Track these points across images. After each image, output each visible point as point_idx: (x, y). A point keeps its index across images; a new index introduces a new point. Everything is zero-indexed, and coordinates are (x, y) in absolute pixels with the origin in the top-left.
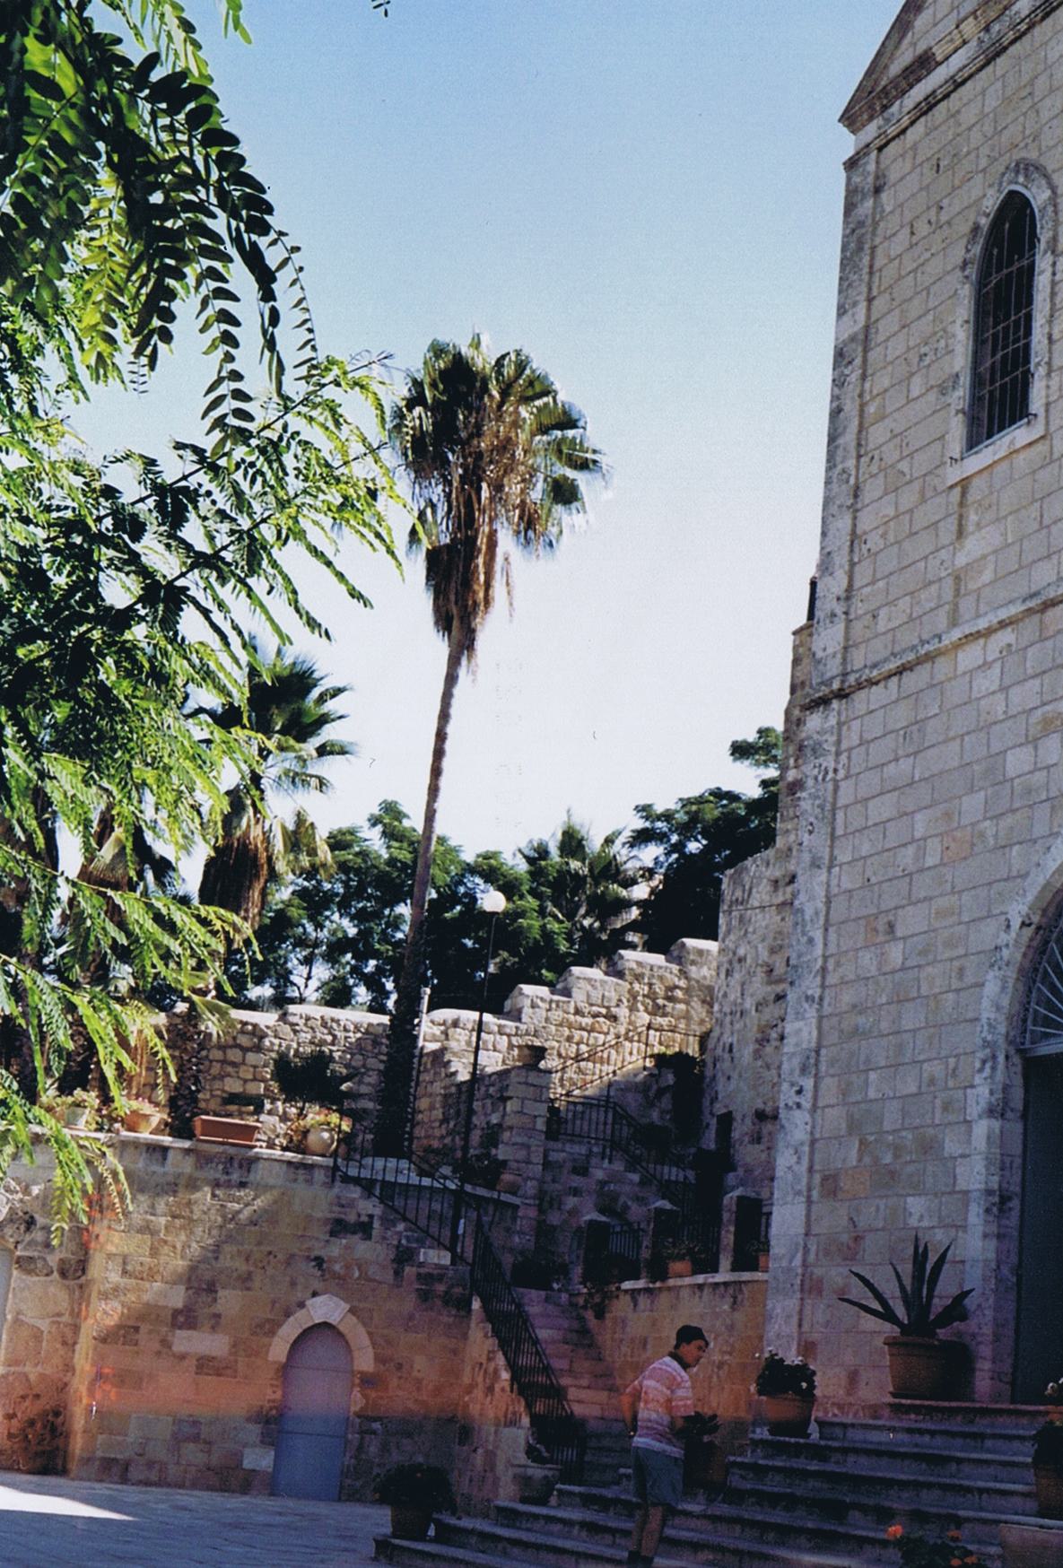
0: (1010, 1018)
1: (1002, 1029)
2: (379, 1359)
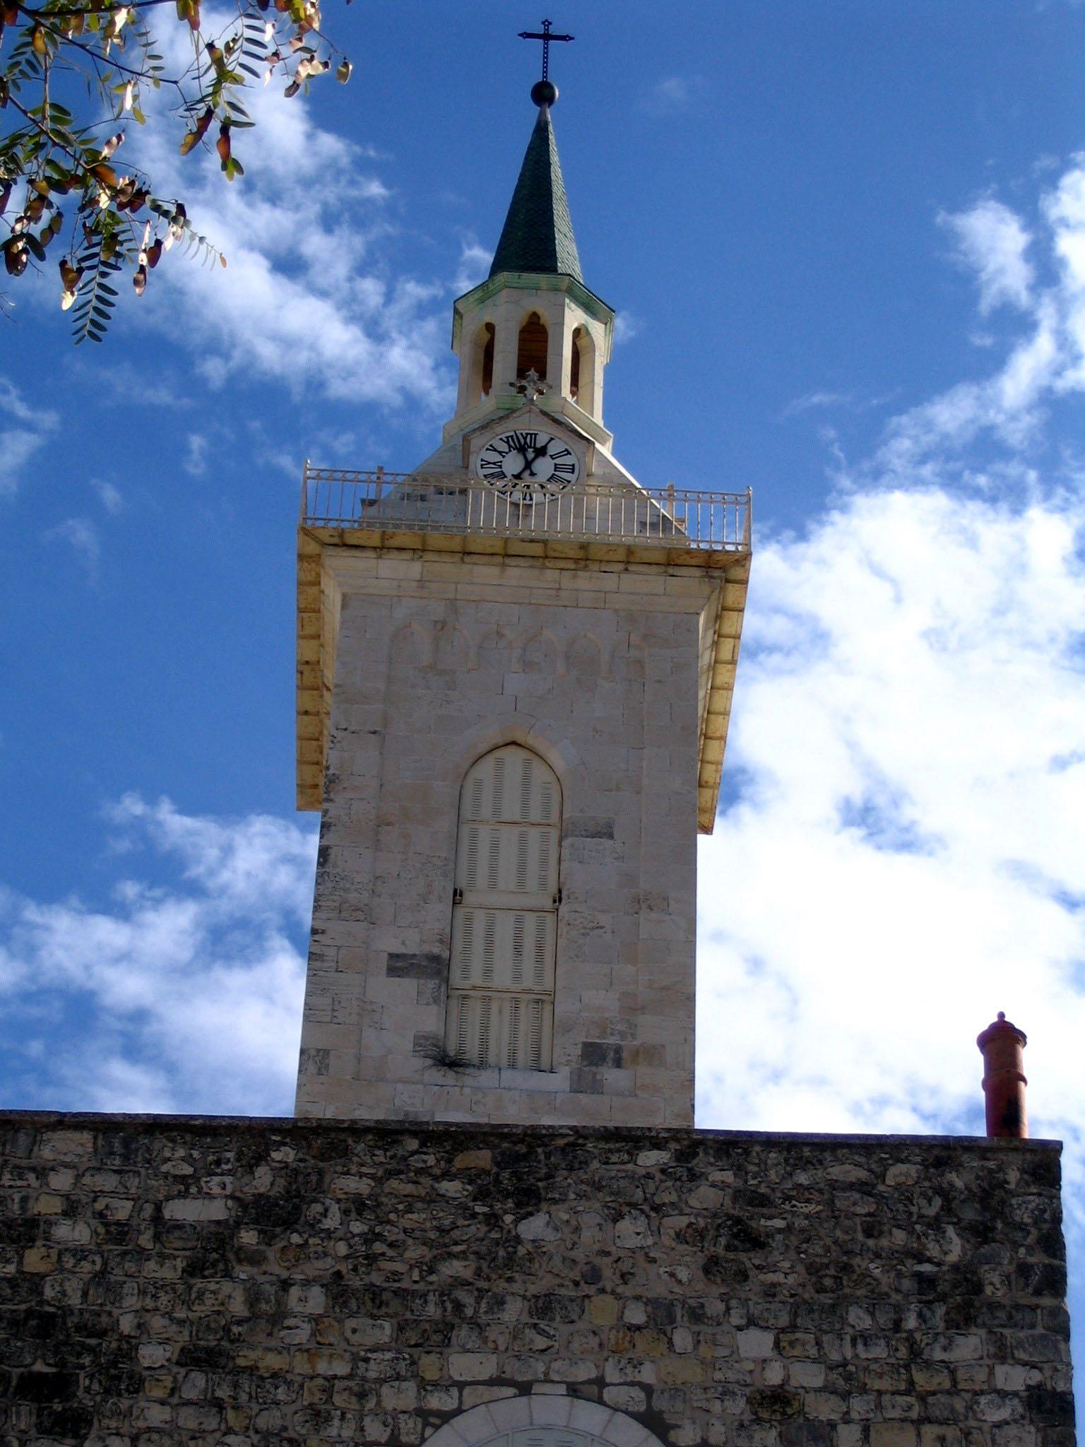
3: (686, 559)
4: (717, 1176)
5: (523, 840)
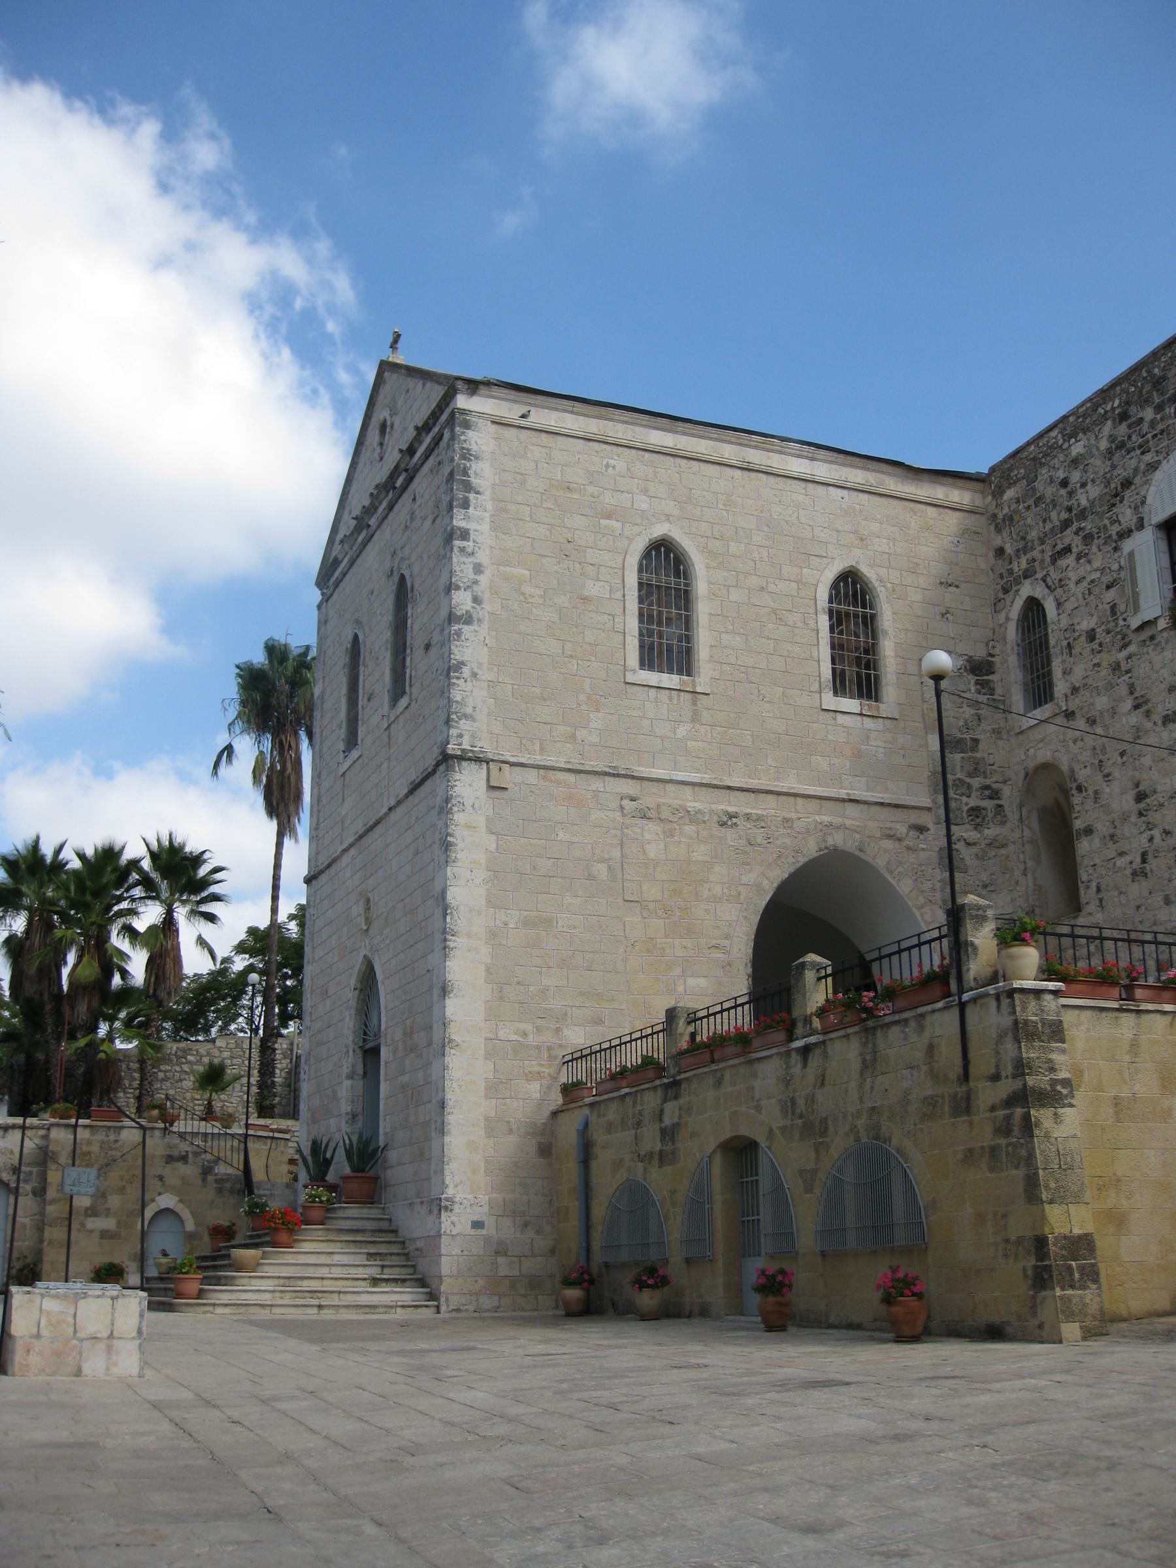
0: (354, 1032)
1: (351, 1038)
2: (197, 1224)
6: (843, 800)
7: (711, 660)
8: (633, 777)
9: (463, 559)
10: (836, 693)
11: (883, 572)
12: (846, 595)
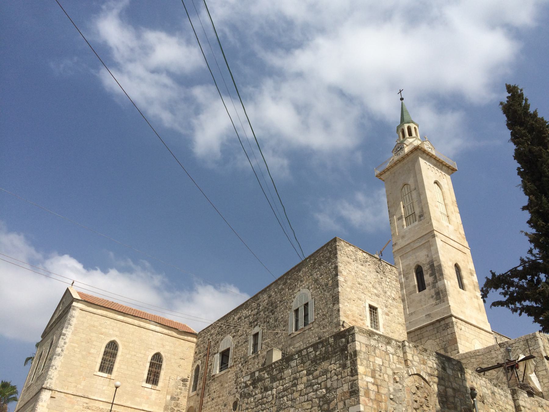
3: (413, 151)
4: (312, 259)
5: (409, 195)
6: (141, 410)
7: (117, 371)
8: (88, 398)
9: (62, 341)
10: (147, 382)
11: (166, 354)
12: (156, 359)
